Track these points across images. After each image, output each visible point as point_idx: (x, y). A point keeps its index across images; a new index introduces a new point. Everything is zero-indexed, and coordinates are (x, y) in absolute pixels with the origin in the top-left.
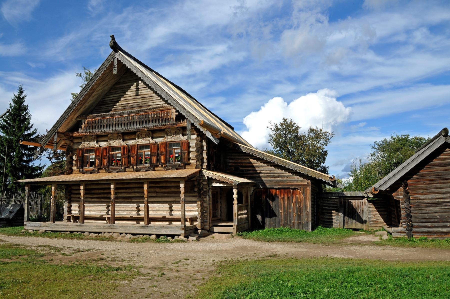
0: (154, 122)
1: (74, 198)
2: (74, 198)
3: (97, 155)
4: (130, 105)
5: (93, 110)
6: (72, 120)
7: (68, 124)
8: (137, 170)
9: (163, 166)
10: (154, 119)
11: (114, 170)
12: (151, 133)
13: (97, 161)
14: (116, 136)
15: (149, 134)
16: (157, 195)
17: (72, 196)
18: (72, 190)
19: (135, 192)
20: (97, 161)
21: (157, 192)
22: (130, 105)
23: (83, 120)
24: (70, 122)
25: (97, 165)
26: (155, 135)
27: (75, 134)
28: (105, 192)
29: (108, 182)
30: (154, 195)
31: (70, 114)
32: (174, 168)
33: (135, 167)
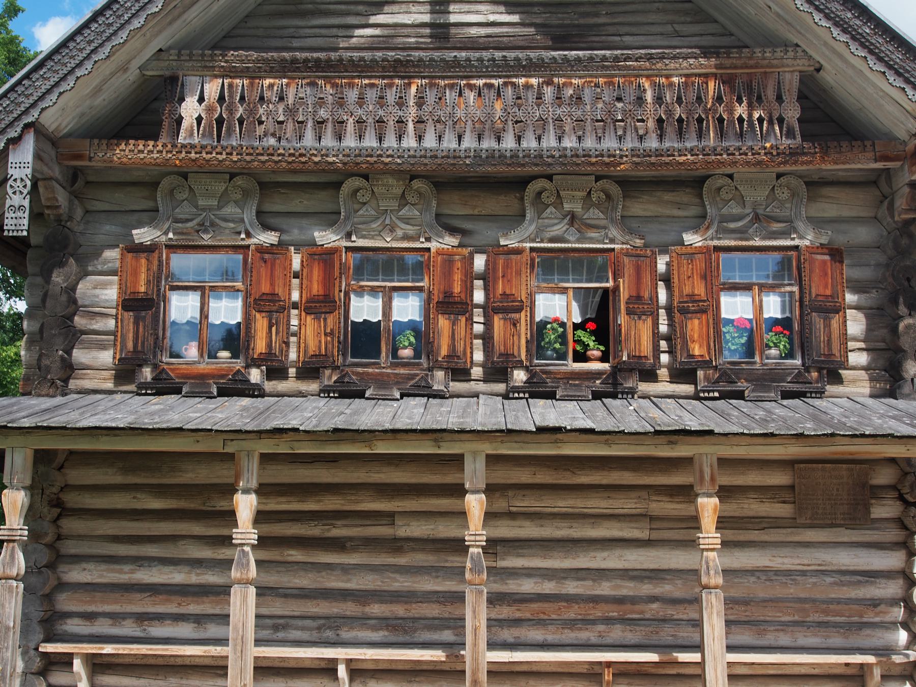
0: (670, 130)
1: (80, 537)
2: (80, 537)
3: (265, 288)
4: (474, 31)
5: (227, 36)
6: (124, 68)
7: (98, 90)
8: (539, 390)
9: (700, 374)
10: (669, 113)
11: (382, 382)
12: (615, 190)
13: (261, 323)
14: (399, 191)
15: (608, 197)
16: (655, 535)
17: (71, 525)
18: (66, 488)
19: (512, 515)
20: (261, 323)
21: (652, 518)
22: (474, 31)
23: (192, 81)
24: (113, 74)
25: (260, 346)
26: (640, 208)
27: (128, 152)
28: (311, 506)
29: (448, 448)
30: (636, 534)
31: (136, 24)
32: (767, 389)
33: (520, 376)
